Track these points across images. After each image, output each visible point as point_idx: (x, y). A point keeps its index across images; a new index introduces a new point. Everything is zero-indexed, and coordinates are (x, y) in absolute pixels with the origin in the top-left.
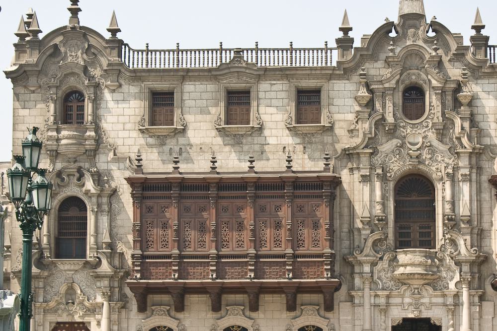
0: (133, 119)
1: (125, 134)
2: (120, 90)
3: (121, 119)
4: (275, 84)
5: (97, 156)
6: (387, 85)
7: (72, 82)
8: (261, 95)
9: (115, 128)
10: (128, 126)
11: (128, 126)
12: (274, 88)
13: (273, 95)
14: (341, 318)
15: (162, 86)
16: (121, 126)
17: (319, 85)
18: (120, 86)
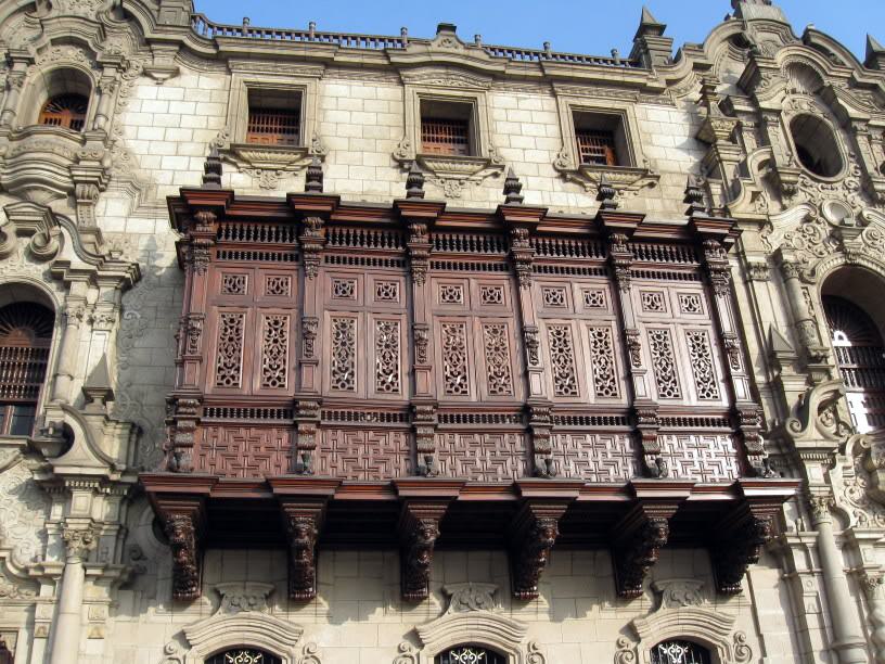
0: (201, 136)
1: (181, 163)
2: (176, 81)
3: (173, 134)
4: (525, 99)
5: (101, 204)
6: (763, 105)
7: (71, 56)
8: (497, 114)
9: (153, 150)
10: (187, 148)
11: (187, 148)
12: (523, 104)
13: (524, 116)
14: (760, 613)
15: (277, 78)
16: (171, 148)
17: (618, 105)
18: (176, 73)
